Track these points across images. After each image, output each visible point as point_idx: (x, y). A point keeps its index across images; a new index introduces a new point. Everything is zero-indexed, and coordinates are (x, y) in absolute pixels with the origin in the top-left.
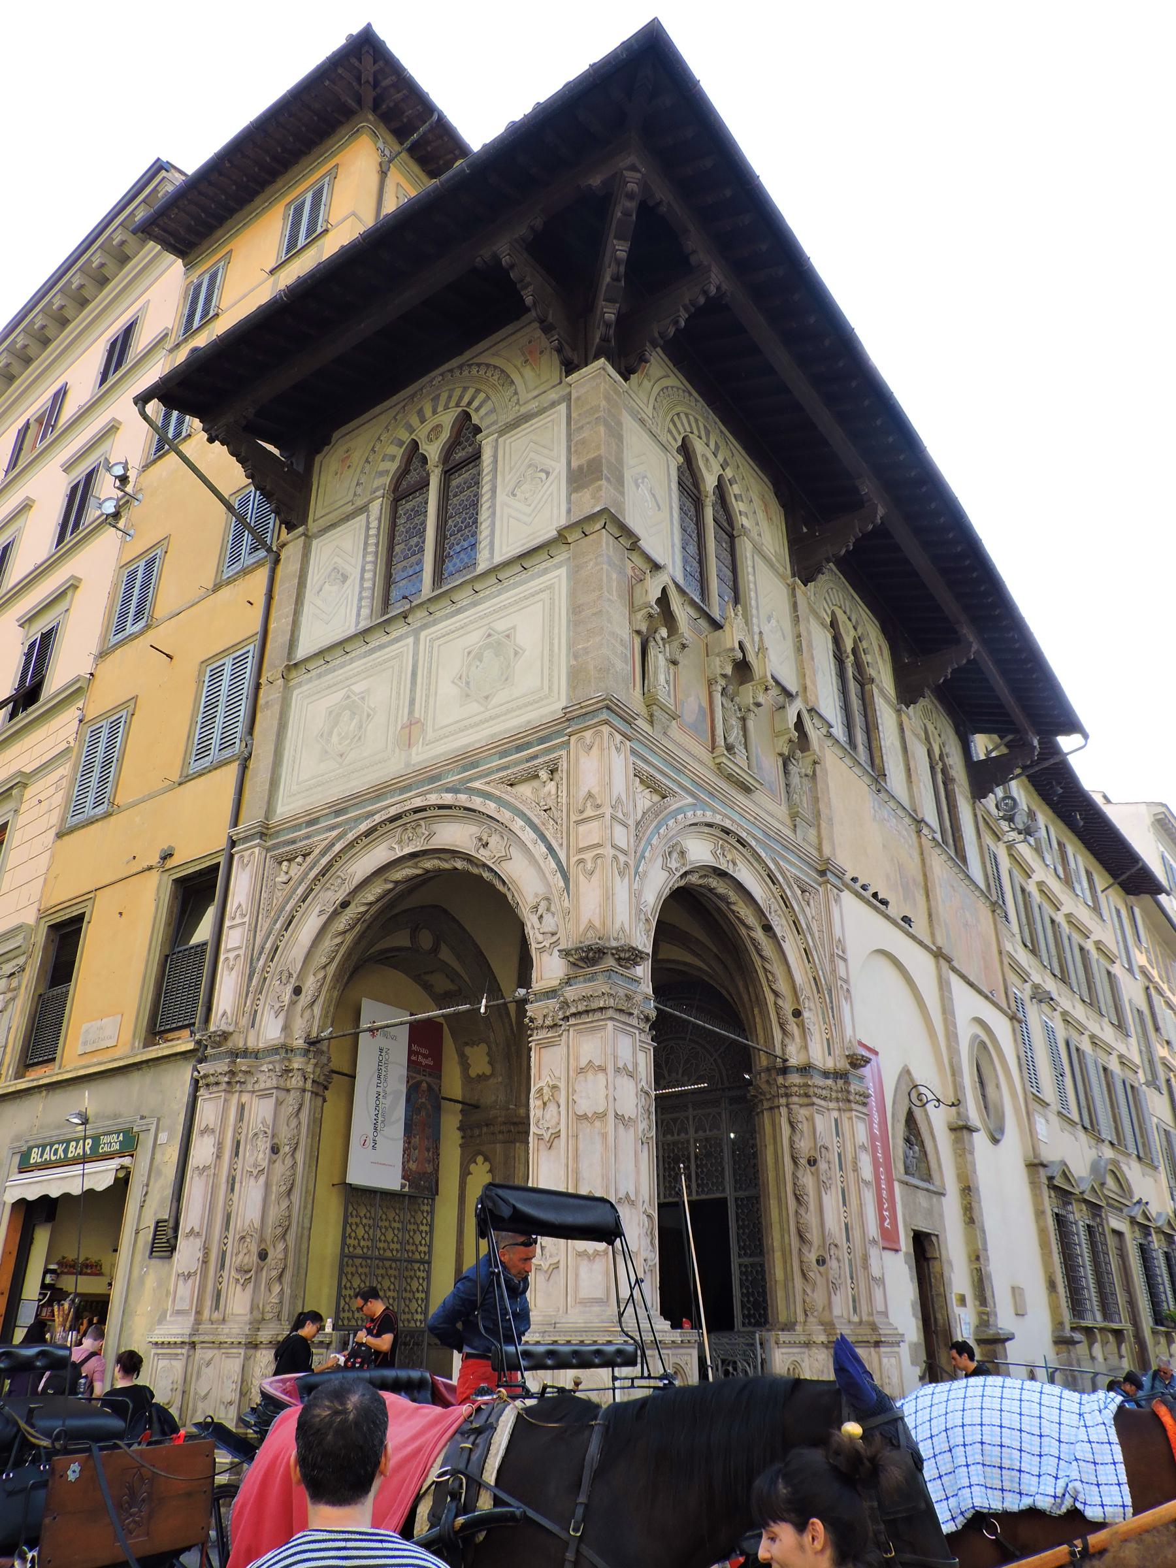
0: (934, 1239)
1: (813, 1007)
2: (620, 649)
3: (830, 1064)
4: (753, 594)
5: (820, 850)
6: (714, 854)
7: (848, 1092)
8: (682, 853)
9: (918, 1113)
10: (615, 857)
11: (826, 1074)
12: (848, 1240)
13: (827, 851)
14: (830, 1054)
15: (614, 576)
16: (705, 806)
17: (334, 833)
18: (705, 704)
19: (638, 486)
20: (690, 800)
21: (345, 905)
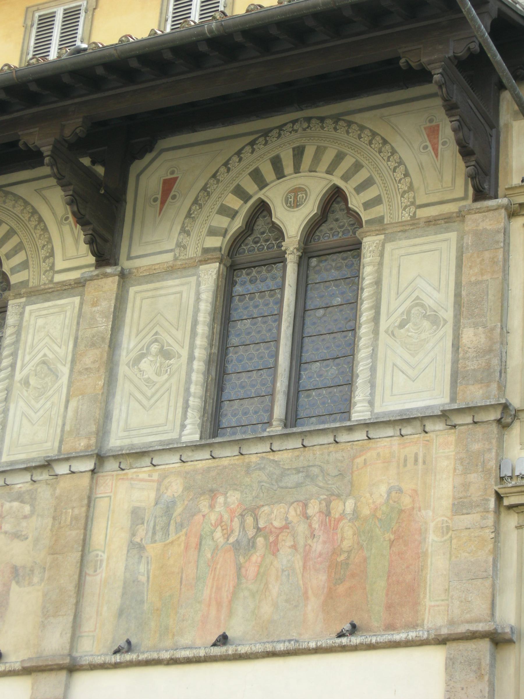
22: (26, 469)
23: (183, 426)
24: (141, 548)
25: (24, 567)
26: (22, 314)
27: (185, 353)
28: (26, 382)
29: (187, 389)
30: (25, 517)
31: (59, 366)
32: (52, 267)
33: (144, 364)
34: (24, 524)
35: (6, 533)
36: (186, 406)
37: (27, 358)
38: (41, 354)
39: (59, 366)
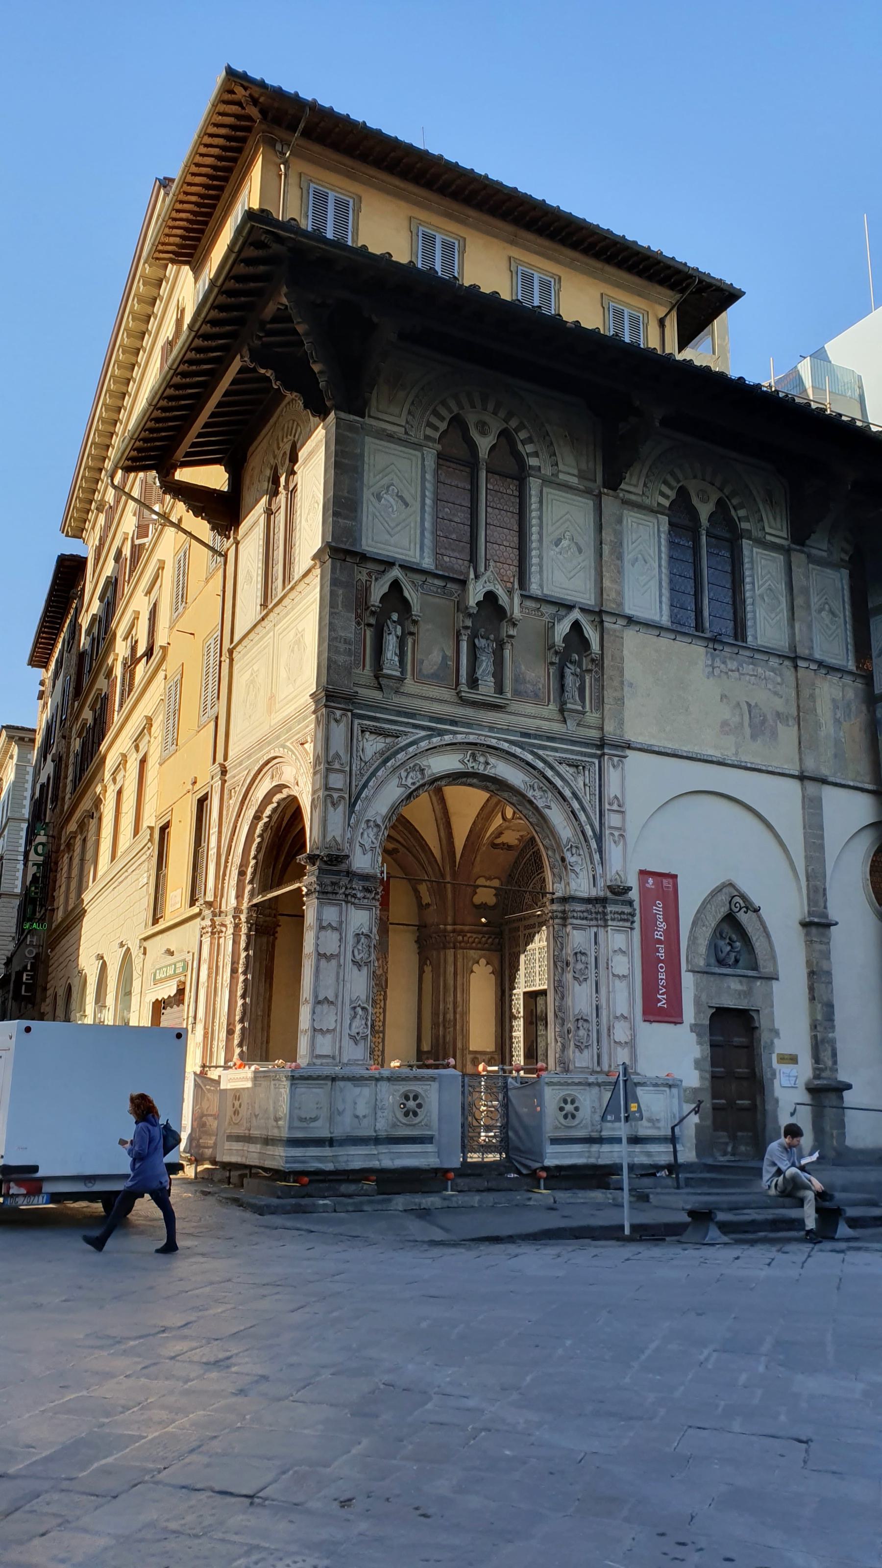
0: (754, 1015)
1: (582, 853)
2: (342, 647)
3: (594, 893)
4: (534, 529)
5: (602, 729)
6: (462, 762)
7: (605, 914)
8: (422, 771)
9: (743, 917)
10: (331, 796)
11: (589, 901)
12: (597, 1016)
13: (609, 727)
14: (594, 886)
15: (340, 592)
16: (441, 733)
17: (246, 772)
18: (449, 653)
19: (379, 498)
20: (423, 733)
21: (257, 817)
22: (779, 656)
23: (848, 660)
24: (840, 722)
25: (783, 714)
26: (752, 551)
27: (842, 615)
28: (762, 597)
29: (846, 639)
30: (778, 684)
31: (780, 597)
32: (764, 529)
33: (824, 614)
34: (779, 687)
35: (770, 689)
36: (847, 650)
37: (760, 583)
38: (767, 584)
39: (780, 597)
